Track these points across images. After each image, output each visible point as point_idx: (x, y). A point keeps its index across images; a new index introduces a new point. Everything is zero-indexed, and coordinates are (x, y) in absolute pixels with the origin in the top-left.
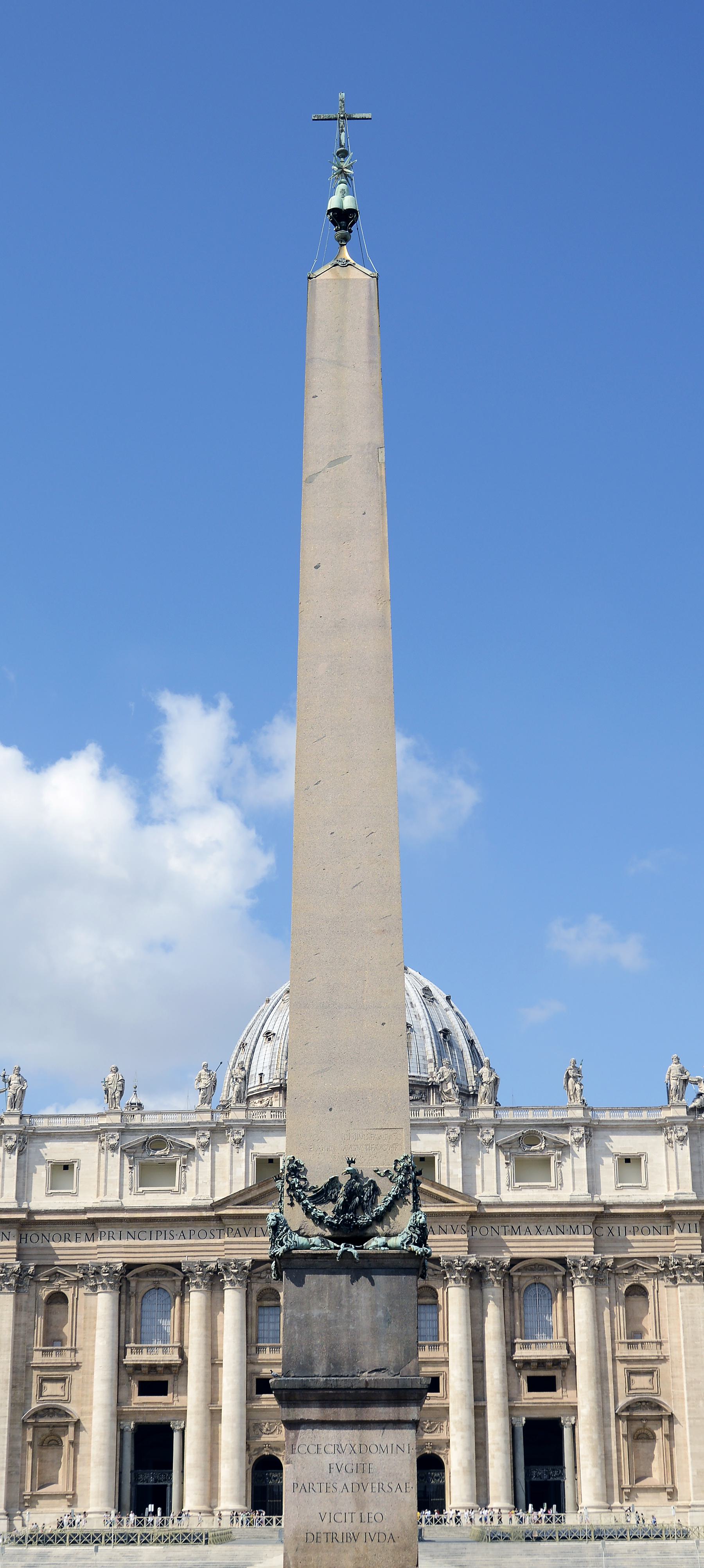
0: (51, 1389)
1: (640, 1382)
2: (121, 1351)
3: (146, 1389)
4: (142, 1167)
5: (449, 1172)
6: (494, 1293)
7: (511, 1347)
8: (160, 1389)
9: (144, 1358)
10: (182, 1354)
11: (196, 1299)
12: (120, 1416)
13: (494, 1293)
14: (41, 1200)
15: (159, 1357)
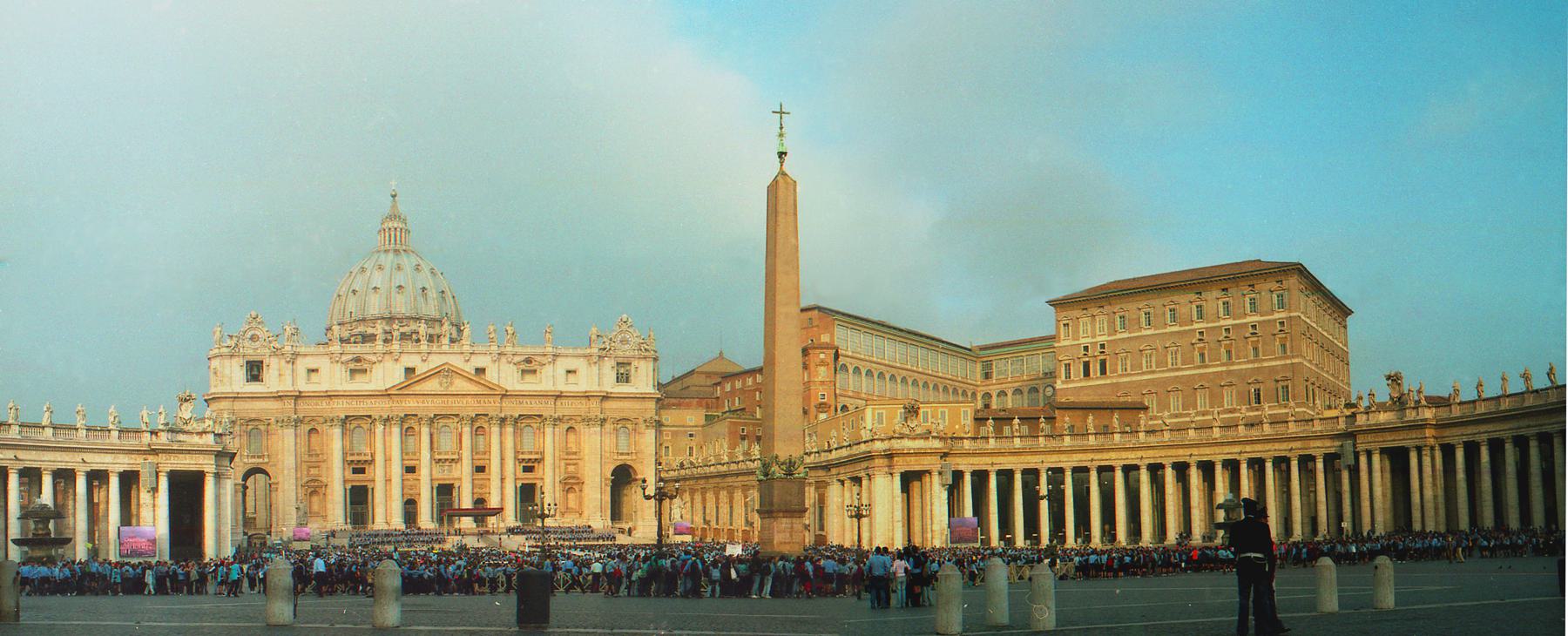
0: (313, 471)
1: (571, 468)
2: (345, 454)
3: (355, 471)
4: (353, 372)
5: (491, 376)
6: (509, 429)
7: (516, 453)
8: (362, 471)
9: (356, 458)
10: (373, 455)
11: (379, 428)
12: (345, 481)
13: (509, 429)
14: (303, 386)
15: (363, 458)
